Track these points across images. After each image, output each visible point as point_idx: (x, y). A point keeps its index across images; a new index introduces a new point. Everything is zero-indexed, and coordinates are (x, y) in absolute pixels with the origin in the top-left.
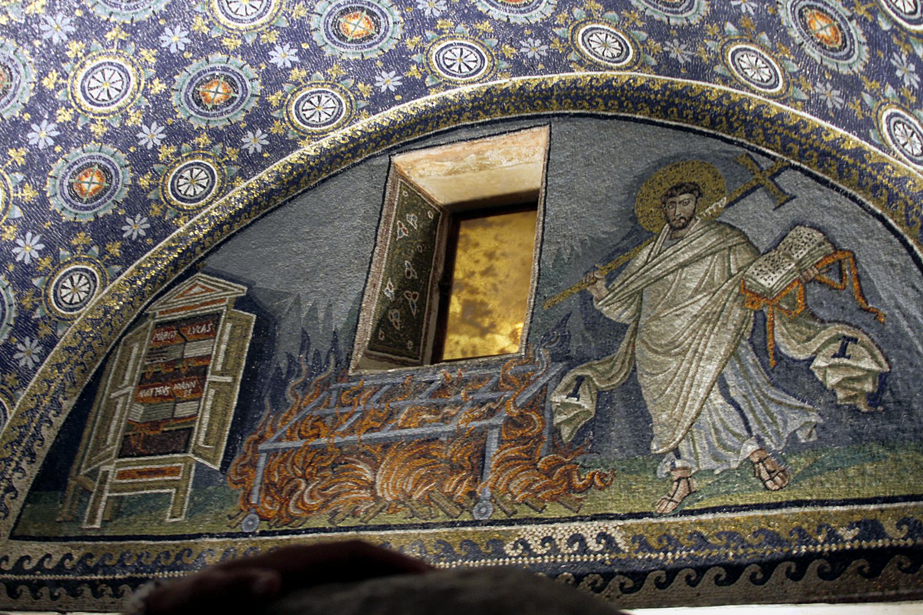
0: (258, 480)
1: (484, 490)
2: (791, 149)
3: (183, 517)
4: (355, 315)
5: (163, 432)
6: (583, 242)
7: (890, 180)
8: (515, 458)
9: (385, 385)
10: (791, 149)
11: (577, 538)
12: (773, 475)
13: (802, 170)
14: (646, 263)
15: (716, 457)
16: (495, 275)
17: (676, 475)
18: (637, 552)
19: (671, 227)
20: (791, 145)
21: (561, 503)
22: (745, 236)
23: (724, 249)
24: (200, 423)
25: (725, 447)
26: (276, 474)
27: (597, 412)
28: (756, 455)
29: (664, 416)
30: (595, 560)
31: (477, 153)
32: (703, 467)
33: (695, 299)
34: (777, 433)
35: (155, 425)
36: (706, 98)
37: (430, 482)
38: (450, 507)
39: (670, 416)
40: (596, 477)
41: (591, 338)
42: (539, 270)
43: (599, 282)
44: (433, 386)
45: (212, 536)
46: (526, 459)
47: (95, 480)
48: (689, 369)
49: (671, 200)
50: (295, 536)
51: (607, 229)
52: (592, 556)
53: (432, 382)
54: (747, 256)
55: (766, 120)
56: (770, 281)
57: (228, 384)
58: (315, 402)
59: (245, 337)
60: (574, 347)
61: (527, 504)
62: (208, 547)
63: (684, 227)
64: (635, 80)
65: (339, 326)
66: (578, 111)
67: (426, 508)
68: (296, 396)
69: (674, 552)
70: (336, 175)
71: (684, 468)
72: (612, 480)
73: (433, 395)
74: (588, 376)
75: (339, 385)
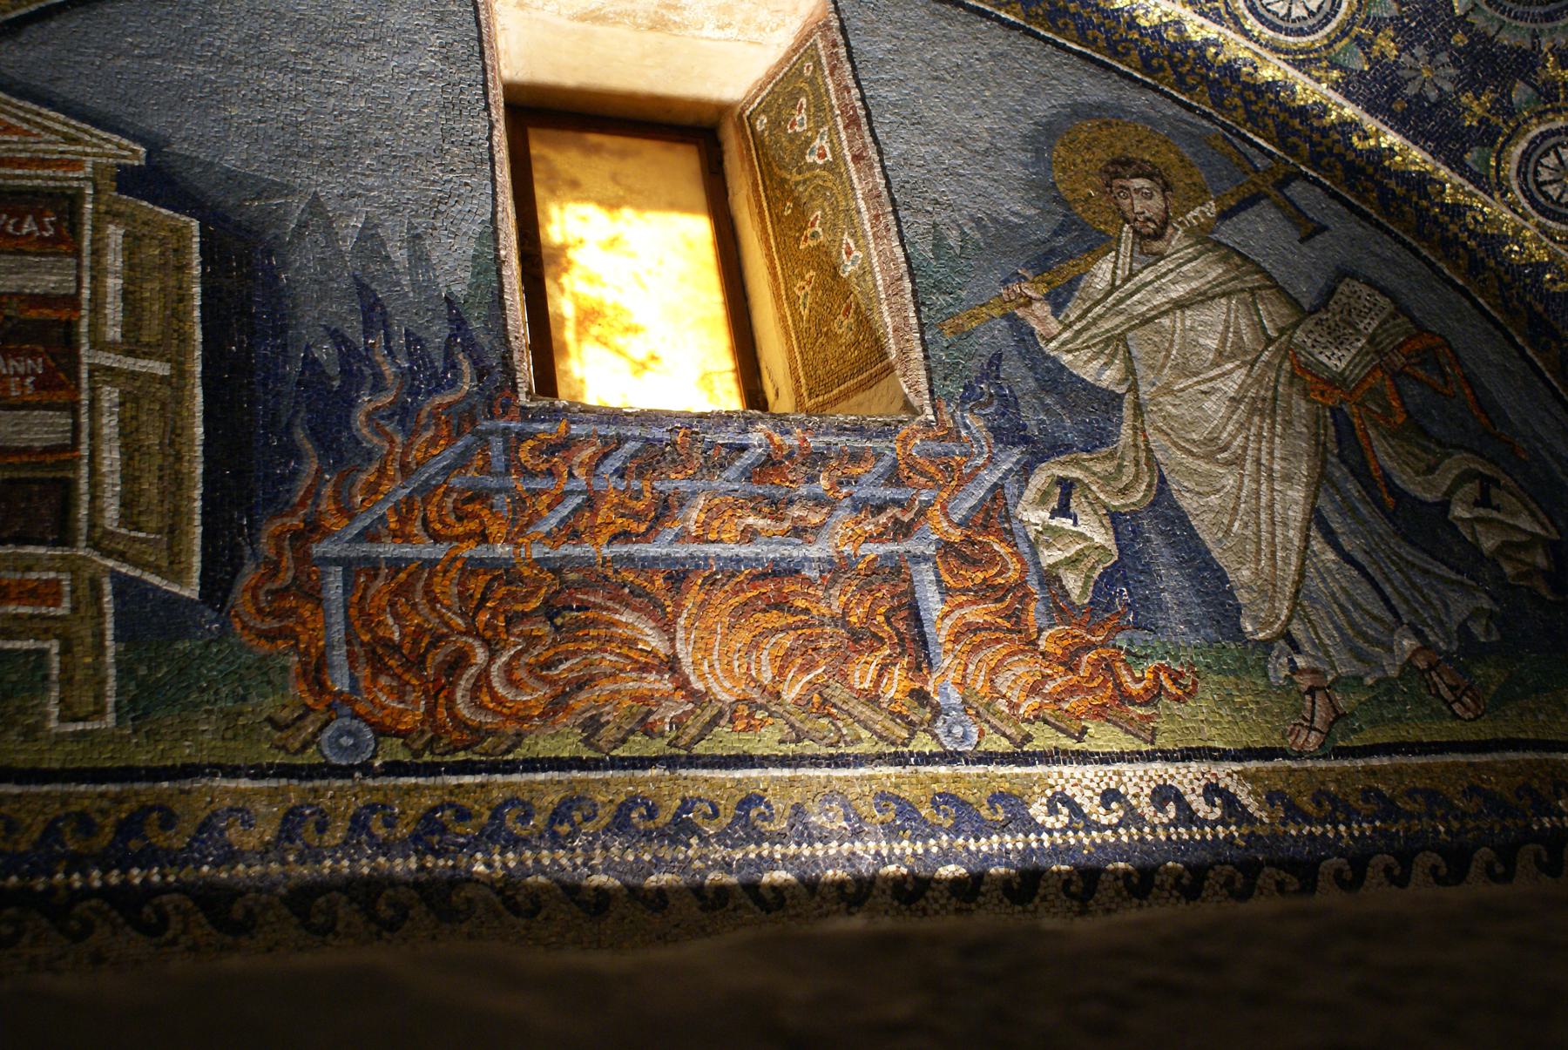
0: (338, 632)
2: (1296, 146)
3: (110, 719)
6: (978, 222)
7: (1472, 234)
9: (627, 439)
10: (1296, 146)
11: (1163, 795)
12: (1459, 693)
14: (1113, 288)
15: (1360, 656)
17: (1305, 682)
19: (1136, 232)
20: (1293, 139)
21: (1115, 724)
22: (1269, 277)
23: (1242, 290)
24: (94, 472)
25: (1365, 636)
27: (1121, 551)
28: (1420, 657)
30: (1215, 836)
32: (1342, 670)
34: (1441, 623)
36: (1133, 19)
38: (881, 721)
39: (1257, 573)
41: (1058, 409)
42: (908, 259)
44: (747, 458)
45: (233, 772)
46: (1009, 631)
48: (1257, 493)
49: (1118, 182)
50: (499, 778)
51: (1017, 208)
52: (1207, 829)
53: (743, 448)
54: (1285, 311)
55: (1246, 86)
56: (1336, 361)
58: (450, 454)
59: (182, 268)
60: (1032, 419)
61: (1046, 722)
62: (228, 802)
63: (1158, 235)
67: (824, 721)
68: (379, 431)
71: (1314, 671)
72: (1195, 683)
73: (749, 475)
74: (1078, 480)
75: (502, 424)
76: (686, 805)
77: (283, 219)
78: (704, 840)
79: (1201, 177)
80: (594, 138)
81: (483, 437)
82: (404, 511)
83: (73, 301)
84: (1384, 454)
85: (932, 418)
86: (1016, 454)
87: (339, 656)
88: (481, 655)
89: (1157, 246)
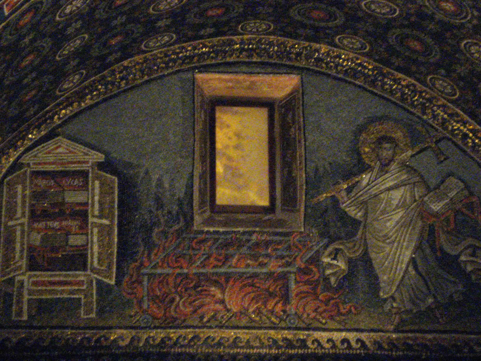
0: (145, 293)
1: (291, 309)
4: (190, 186)
5: (63, 255)
6: (330, 164)
8: (308, 292)
13: (453, 142)
14: (368, 184)
15: (414, 304)
16: (243, 150)
17: (394, 311)
18: (377, 350)
19: (381, 164)
22: (422, 177)
25: (418, 298)
26: (157, 290)
29: (385, 278)
31: (252, 82)
33: (397, 211)
35: (54, 249)
37: (257, 302)
38: (273, 319)
40: (352, 308)
43: (343, 192)
44: (251, 243)
45: (120, 328)
47: (14, 286)
56: (436, 207)
57: (108, 226)
58: (175, 245)
59: (113, 193)
63: (388, 165)
64: (358, 59)
65: (182, 195)
66: (318, 69)
69: (396, 352)
70: (154, 79)
73: (249, 248)
76: (222, 338)
77: (138, 177)
78: (224, 347)
79: (408, 140)
80: (235, 109)
81: (184, 239)
82: (163, 261)
83: (86, 204)
84: (443, 239)
85: (303, 230)
86: (326, 241)
87: (145, 299)
88: (178, 299)
89: (387, 169)
